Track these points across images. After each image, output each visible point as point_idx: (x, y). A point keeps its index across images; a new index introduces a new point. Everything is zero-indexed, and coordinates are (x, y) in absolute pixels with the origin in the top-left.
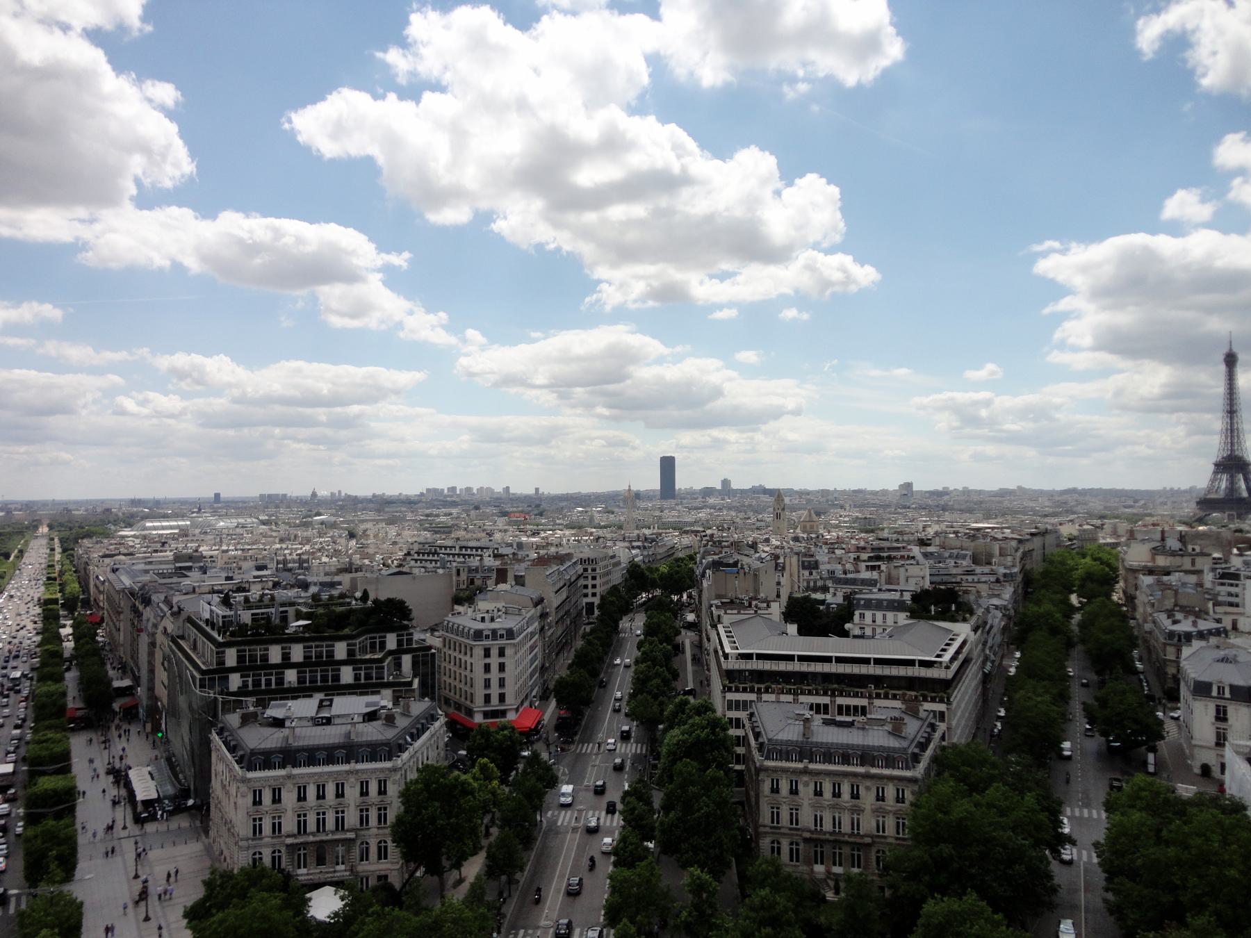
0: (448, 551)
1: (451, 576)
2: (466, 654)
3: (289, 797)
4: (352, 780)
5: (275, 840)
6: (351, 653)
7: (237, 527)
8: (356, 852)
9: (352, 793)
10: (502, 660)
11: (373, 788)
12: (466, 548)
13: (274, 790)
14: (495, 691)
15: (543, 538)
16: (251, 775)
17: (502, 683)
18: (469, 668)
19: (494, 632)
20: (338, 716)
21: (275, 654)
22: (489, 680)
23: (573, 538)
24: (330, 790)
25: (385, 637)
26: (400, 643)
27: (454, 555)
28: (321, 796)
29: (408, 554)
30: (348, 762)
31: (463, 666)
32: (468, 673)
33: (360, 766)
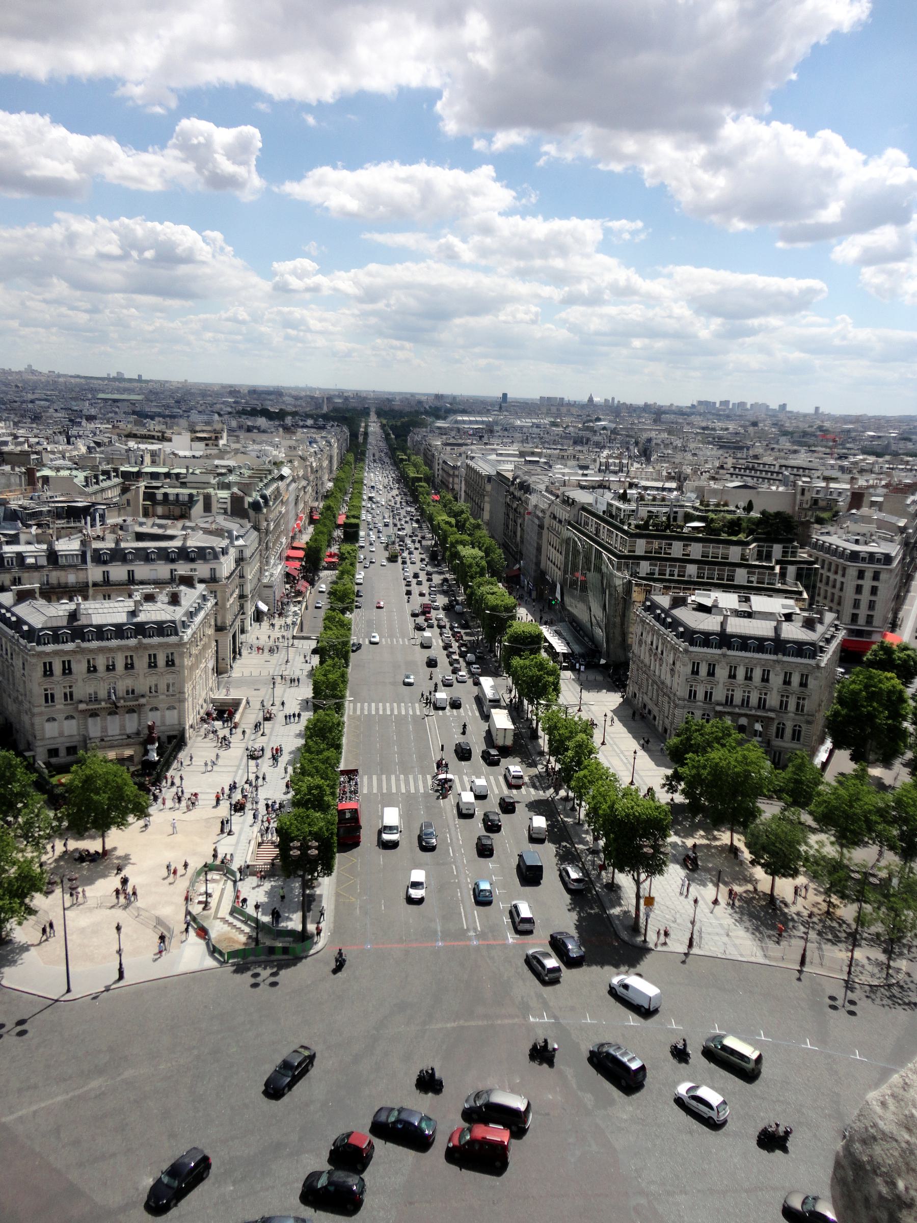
0: (767, 468)
1: (795, 494)
2: (836, 573)
3: (722, 673)
4: (778, 669)
5: (706, 706)
6: (743, 557)
7: (532, 427)
8: (773, 729)
9: (776, 680)
10: (875, 584)
11: (796, 680)
12: (787, 467)
13: (710, 665)
14: (863, 612)
15: (853, 463)
16: (692, 649)
17: (872, 605)
18: (838, 585)
19: (872, 555)
20: (759, 612)
21: (677, 550)
22: (859, 600)
23: (887, 466)
24: (757, 674)
25: (772, 547)
26: (785, 553)
27: (772, 473)
28: (748, 678)
29: (722, 467)
30: (776, 653)
31: (831, 583)
32: (836, 591)
33: (786, 659)
